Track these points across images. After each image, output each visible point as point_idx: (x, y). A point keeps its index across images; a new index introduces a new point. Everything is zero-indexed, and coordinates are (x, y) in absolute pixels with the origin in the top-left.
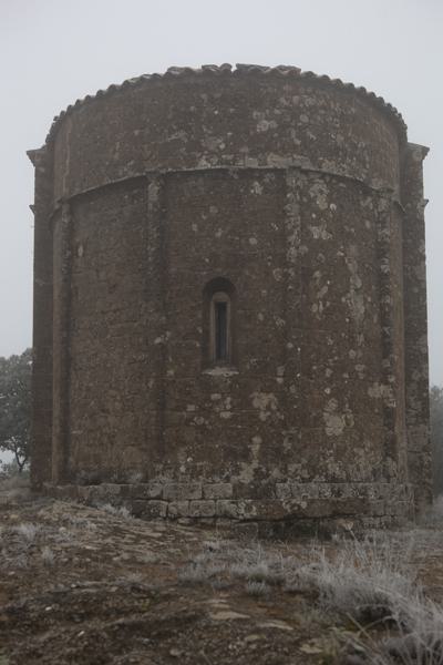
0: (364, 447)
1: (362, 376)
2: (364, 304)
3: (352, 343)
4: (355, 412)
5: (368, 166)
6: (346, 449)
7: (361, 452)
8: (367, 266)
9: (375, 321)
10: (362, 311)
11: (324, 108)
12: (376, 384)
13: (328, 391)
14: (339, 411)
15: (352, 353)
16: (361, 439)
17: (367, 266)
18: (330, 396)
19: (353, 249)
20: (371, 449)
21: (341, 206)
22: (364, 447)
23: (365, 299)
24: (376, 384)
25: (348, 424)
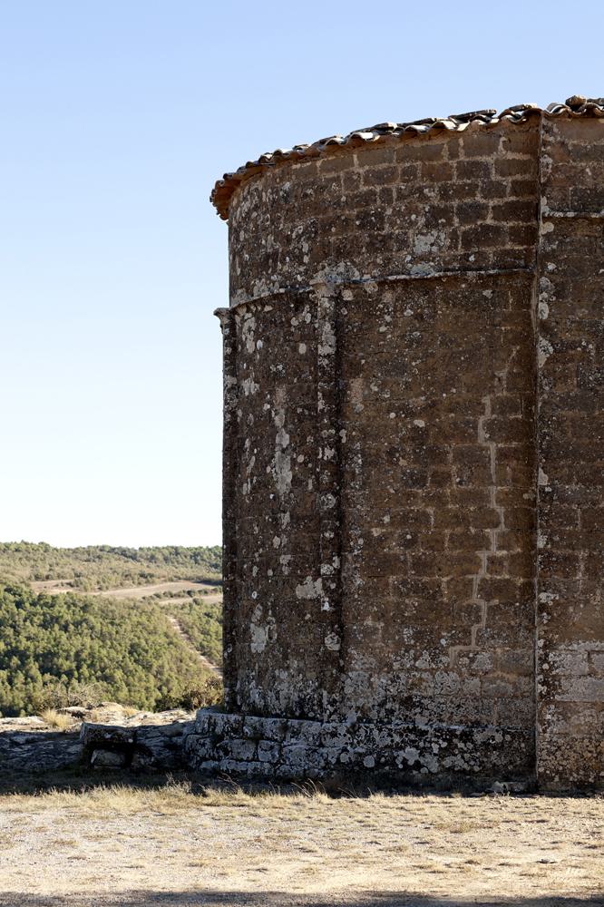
0: (288, 668)
1: (286, 570)
2: (292, 469)
3: (276, 523)
4: (279, 621)
5: (306, 259)
6: (267, 670)
7: (284, 675)
8: (299, 410)
9: (310, 487)
10: (289, 480)
11: (256, 208)
12: (309, 578)
13: (255, 595)
14: (263, 622)
15: (276, 541)
16: (286, 657)
17: (299, 410)
18: (257, 601)
19: (281, 394)
20: (300, 671)
21: (267, 340)
22: (288, 668)
23: (294, 461)
24: (309, 578)
25: (270, 638)
